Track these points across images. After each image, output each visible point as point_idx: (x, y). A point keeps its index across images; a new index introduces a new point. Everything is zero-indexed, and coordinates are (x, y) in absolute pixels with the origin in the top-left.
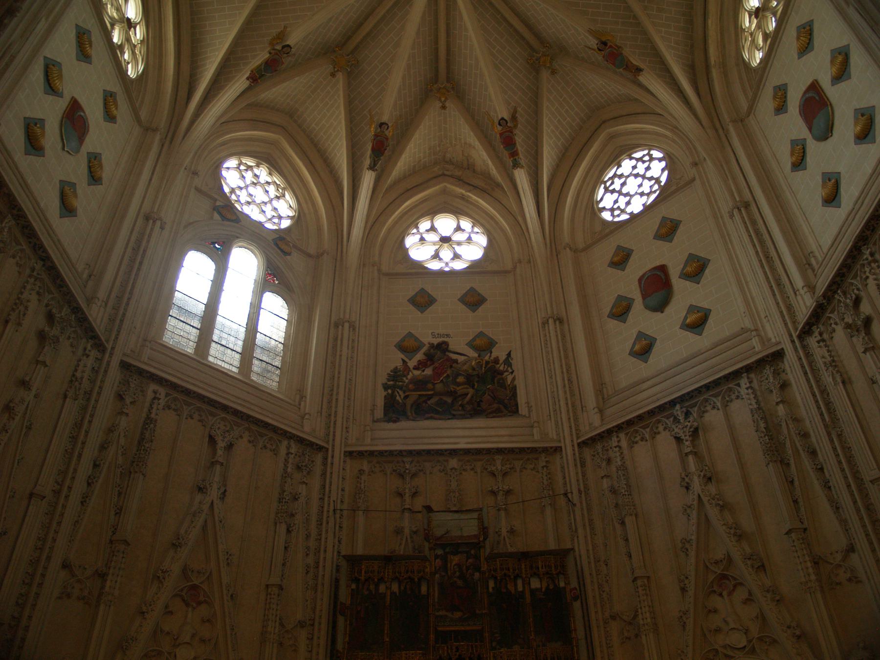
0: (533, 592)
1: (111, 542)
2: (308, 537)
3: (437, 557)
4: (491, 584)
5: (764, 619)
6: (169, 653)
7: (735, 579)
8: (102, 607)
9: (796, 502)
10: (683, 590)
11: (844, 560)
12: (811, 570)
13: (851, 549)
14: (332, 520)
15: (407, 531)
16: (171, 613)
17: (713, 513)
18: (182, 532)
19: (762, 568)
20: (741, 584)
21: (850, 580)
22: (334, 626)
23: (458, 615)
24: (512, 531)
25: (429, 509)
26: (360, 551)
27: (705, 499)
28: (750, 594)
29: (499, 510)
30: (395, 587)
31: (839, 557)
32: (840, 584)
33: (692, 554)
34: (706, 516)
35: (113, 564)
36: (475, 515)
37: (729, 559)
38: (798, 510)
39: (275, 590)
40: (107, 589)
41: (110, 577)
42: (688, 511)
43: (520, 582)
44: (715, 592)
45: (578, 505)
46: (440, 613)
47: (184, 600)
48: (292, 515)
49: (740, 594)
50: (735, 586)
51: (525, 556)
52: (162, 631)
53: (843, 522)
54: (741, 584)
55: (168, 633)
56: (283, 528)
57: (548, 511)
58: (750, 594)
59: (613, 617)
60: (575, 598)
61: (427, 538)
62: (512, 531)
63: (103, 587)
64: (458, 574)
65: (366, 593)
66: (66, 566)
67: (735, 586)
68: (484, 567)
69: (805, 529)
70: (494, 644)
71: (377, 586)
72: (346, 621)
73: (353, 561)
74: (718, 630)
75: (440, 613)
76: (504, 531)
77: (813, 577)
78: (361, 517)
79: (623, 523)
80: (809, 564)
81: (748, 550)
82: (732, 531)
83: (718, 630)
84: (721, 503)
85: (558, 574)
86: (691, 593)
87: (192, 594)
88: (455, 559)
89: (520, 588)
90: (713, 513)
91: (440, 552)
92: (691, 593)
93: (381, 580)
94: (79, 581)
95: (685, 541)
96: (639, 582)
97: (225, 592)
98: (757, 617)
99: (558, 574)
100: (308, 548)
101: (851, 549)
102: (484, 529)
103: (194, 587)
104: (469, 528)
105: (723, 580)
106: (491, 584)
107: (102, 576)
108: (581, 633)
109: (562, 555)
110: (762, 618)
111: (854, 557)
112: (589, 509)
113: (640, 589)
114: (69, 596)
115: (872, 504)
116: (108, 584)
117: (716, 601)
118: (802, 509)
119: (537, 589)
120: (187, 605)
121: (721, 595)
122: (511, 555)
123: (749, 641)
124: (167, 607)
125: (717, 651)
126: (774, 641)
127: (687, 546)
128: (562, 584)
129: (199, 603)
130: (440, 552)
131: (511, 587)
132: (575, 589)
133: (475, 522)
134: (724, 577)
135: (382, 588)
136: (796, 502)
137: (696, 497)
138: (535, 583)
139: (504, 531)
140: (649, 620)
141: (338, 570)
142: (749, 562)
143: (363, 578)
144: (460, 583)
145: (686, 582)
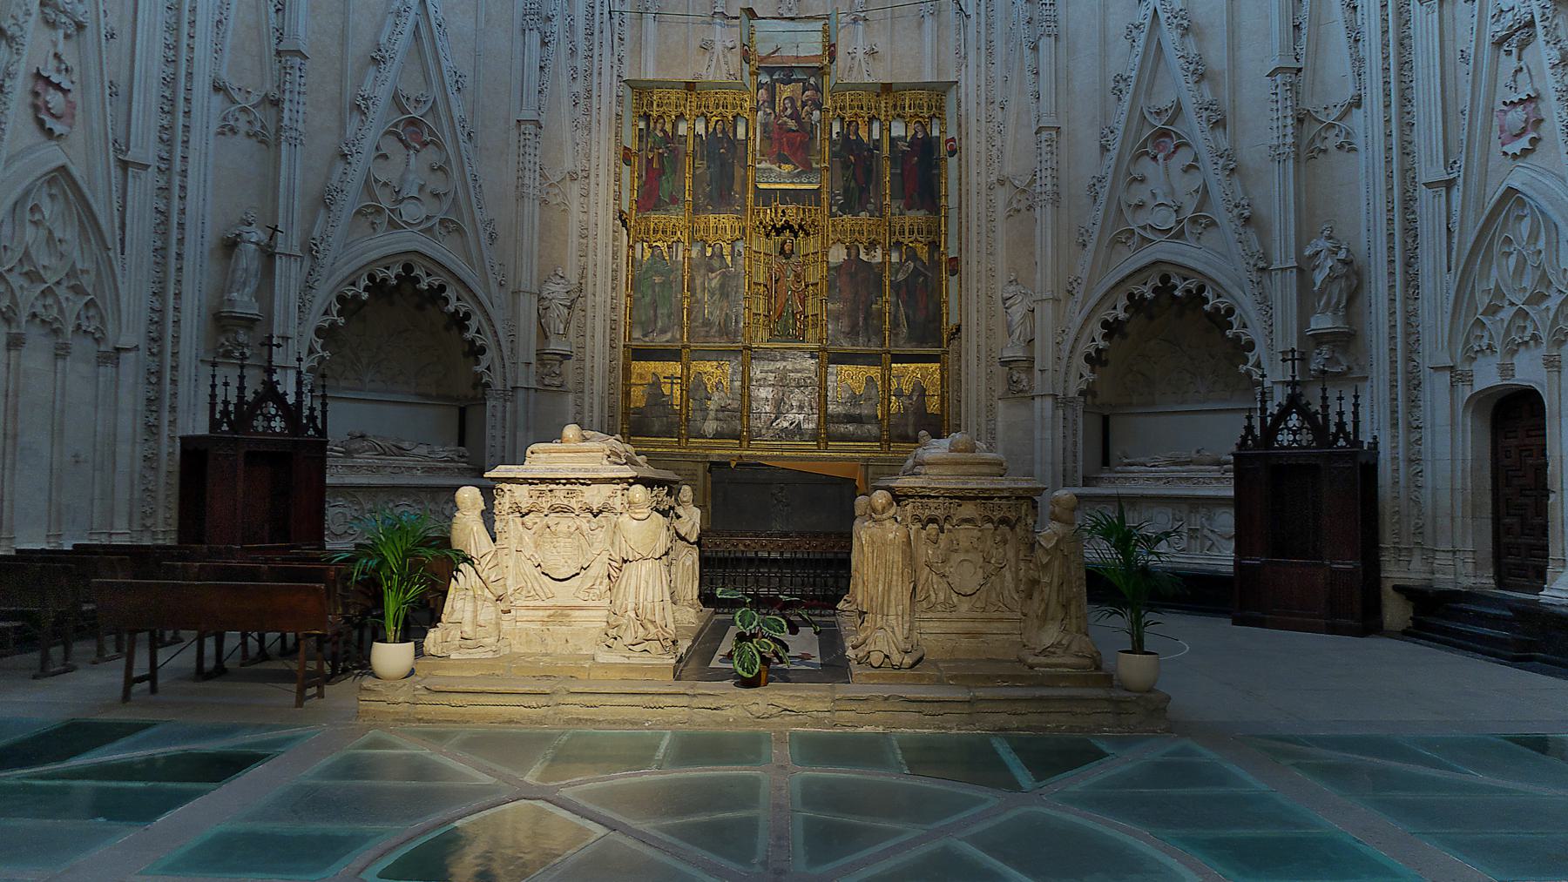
0: (892, 140)
1: (278, 53)
2: (573, 52)
3: (760, 86)
4: (836, 128)
5: (1206, 191)
6: (392, 211)
7: (1179, 136)
8: (284, 146)
9: (1297, 27)
10: (1104, 149)
11: (1340, 119)
12: (1290, 130)
13: (1357, 103)
14: (606, 27)
15: (718, 47)
16: (385, 157)
17: (1170, 36)
18: (383, 40)
19: (1219, 124)
20: (1187, 144)
21: (1340, 147)
22: (618, 179)
23: (787, 168)
24: (872, 53)
25: (751, 13)
26: (650, 76)
27: (1163, 16)
28: (1196, 160)
29: (855, 21)
30: (700, 128)
31: (1335, 113)
32: (1325, 151)
33: (1127, 98)
34: (1159, 43)
35: (288, 86)
36: (819, 25)
37: (1178, 108)
38: (1296, 40)
39: (531, 128)
40: (286, 121)
41: (287, 105)
42: (1135, 32)
43: (876, 125)
44: (1147, 153)
45: (974, 16)
46: (763, 165)
47: (401, 140)
48: (549, 19)
49: (1184, 157)
50: (1177, 147)
51: (887, 88)
52: (376, 181)
53: (1358, 62)
54: (1187, 144)
55: (385, 184)
56: (535, 38)
57: (929, 23)
58: (1196, 160)
59: (1001, 182)
60: (952, 153)
61: (746, 57)
62: (872, 53)
63: (281, 119)
64: (789, 111)
65: (660, 134)
66: (218, 88)
67: (1177, 147)
68: (828, 104)
69: (1300, 70)
70: (834, 209)
71: (675, 127)
72: (633, 172)
73: (641, 89)
74: (1140, 206)
75: (763, 165)
76: (860, 54)
77: (1290, 140)
78: (650, 24)
79: (1035, 48)
80: (1289, 121)
81: (1208, 97)
82: (1192, 68)
83: (1140, 206)
84: (1185, 23)
85: (931, 118)
86: (1114, 154)
87: (412, 130)
88: (786, 91)
89: (876, 136)
90: (1170, 36)
91: (765, 79)
92: (1114, 154)
93: (680, 117)
94: (244, 110)
95: (1121, 79)
96: (1044, 135)
97: (459, 129)
98: (1197, 191)
99: (931, 118)
100: (575, 69)
101: (1357, 103)
102: (831, 51)
103: (412, 122)
104: (808, 45)
105: (1162, 137)
106: (836, 128)
107: (276, 103)
108: (953, 201)
109: (939, 91)
110: (1204, 192)
111: (1358, 114)
112: (989, 26)
113: (1044, 144)
114: (233, 131)
115: (1410, 37)
116: (286, 114)
117: (1147, 167)
118: (1304, 38)
119: (899, 138)
120: (407, 147)
121: (1155, 158)
122: (866, 87)
123: (1179, 222)
124: (377, 149)
125: (1132, 232)
126: (1213, 223)
127: (1122, 85)
128: (936, 133)
129: (425, 144)
130: (765, 79)
131: (863, 134)
132: (953, 139)
133: (819, 37)
134: (1164, 133)
135: (682, 129)
136: (1297, 27)
137: (1150, 12)
138: (898, 130)
139: (860, 54)
140: (1049, 187)
141: (619, 103)
142: (1205, 114)
143: (655, 114)
144: (792, 124)
145: (1111, 137)
